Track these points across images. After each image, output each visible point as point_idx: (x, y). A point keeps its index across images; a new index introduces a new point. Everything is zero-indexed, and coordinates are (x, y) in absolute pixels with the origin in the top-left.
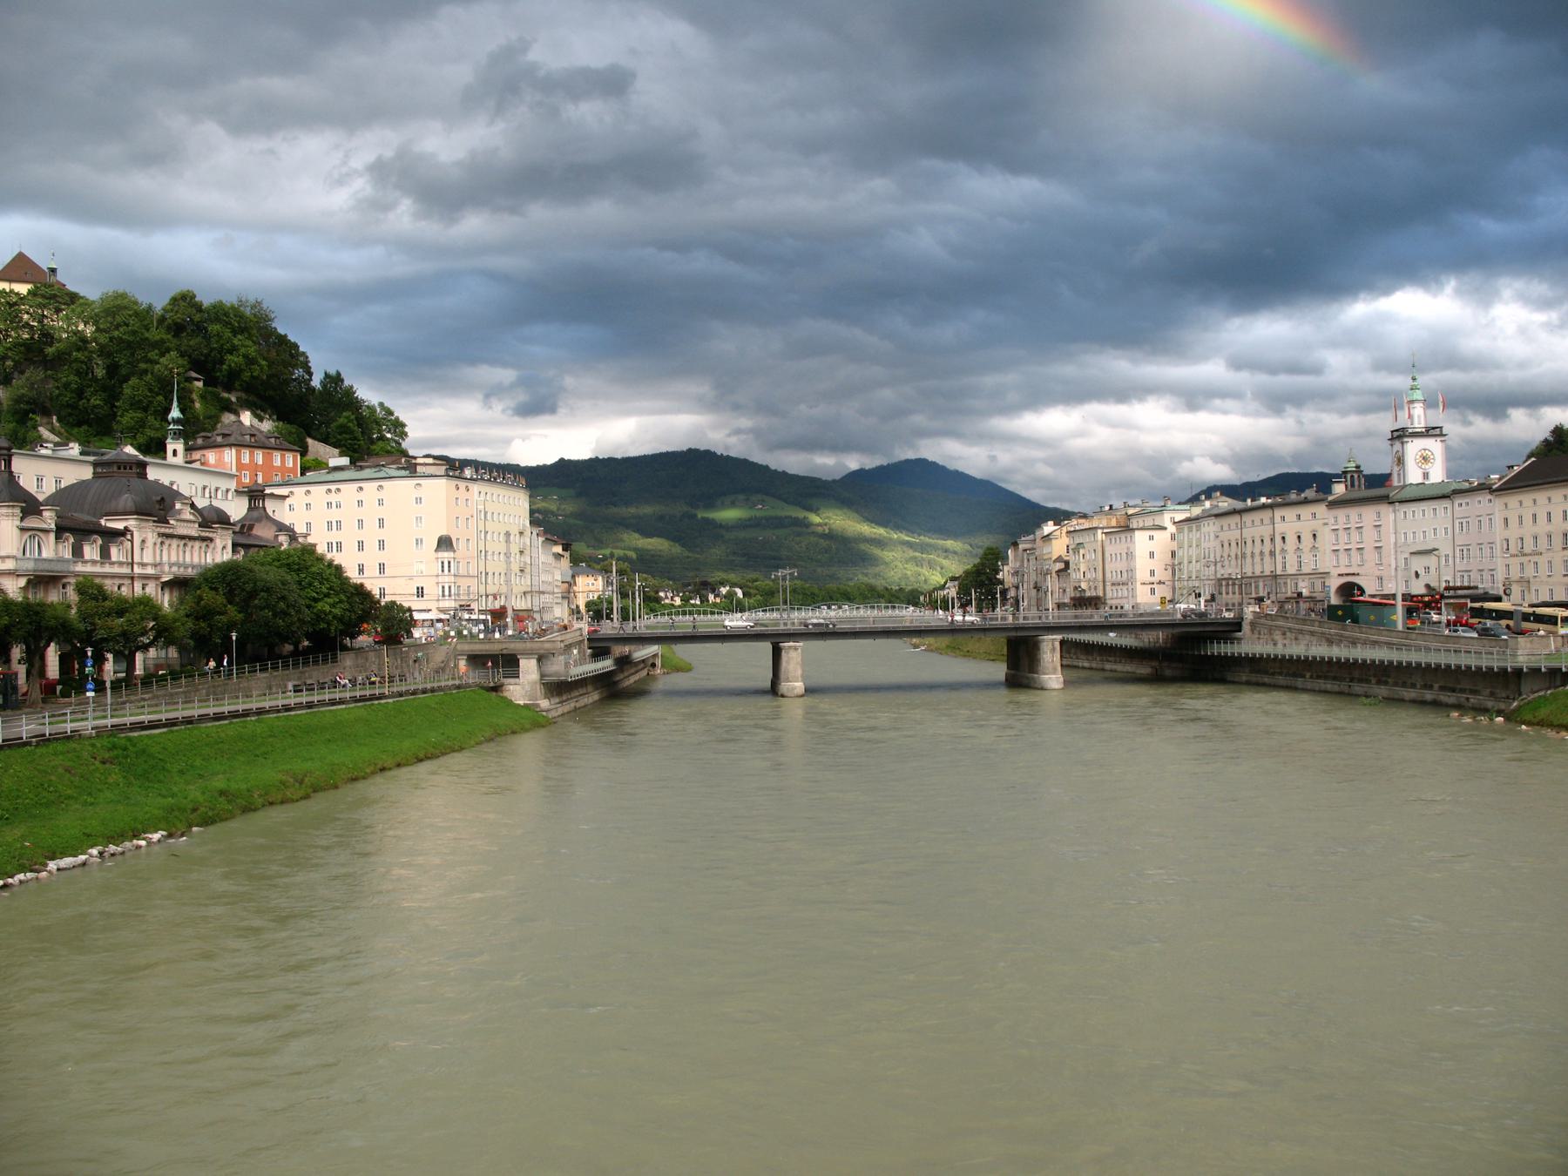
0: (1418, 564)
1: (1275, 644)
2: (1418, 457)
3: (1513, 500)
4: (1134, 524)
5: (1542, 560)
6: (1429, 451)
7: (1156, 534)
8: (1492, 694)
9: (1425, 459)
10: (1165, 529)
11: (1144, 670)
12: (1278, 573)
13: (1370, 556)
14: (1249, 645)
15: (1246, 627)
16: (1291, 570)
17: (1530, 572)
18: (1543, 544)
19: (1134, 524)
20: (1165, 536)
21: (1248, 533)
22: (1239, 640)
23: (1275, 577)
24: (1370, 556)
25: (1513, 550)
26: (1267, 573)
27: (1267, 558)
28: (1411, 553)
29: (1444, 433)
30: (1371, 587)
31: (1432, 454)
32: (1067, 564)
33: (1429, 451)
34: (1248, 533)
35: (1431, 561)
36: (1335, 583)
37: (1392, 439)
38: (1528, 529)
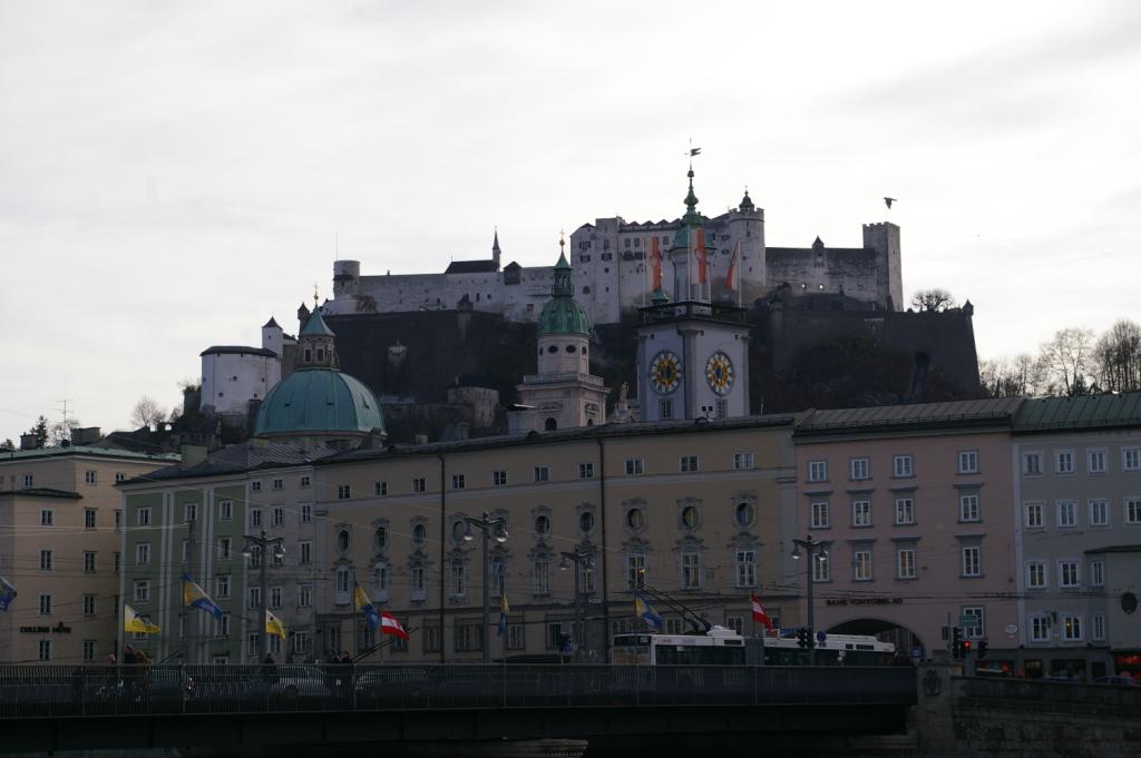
2: (710, 367)
6: (726, 357)
7: (58, 509)
9: (719, 372)
10: (77, 497)
12: (611, 598)
20: (76, 511)
28: (1086, 553)
31: (731, 365)
33: (726, 357)
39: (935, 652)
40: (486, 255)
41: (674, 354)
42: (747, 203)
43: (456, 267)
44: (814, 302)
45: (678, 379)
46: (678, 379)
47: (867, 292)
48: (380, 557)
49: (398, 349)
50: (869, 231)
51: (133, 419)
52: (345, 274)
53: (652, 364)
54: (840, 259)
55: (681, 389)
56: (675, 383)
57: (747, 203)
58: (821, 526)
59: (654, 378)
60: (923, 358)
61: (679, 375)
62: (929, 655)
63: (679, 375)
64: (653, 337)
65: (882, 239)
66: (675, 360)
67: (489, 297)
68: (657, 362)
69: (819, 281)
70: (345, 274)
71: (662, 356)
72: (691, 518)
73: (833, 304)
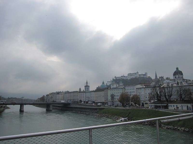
0: (87, 98)
1: (73, 106)
3: (96, 93)
4: (60, 93)
5: (98, 98)
8: (94, 111)
11: (60, 108)
13: (83, 97)
14: (72, 106)
15: (71, 104)
16: (75, 99)
17: (97, 99)
18: (98, 97)
19: (60, 93)
21: (71, 95)
22: (70, 105)
23: (73, 99)
24: (83, 97)
25: (96, 97)
26: (73, 99)
27: (73, 97)
32: (52, 97)
34: (71, 95)
35: (88, 98)
36: (79, 100)
37: (85, 86)
38: (97, 95)
40: (123, 76)
42: (137, 72)
43: (121, 76)
44: (142, 77)
47: (145, 77)
49: (118, 81)
50: (145, 73)
51: (67, 91)
52: (115, 77)
54: (143, 75)
57: (137, 72)
60: (148, 81)
65: (146, 73)
67: (123, 78)
69: (142, 76)
70: (115, 77)
73: (143, 77)
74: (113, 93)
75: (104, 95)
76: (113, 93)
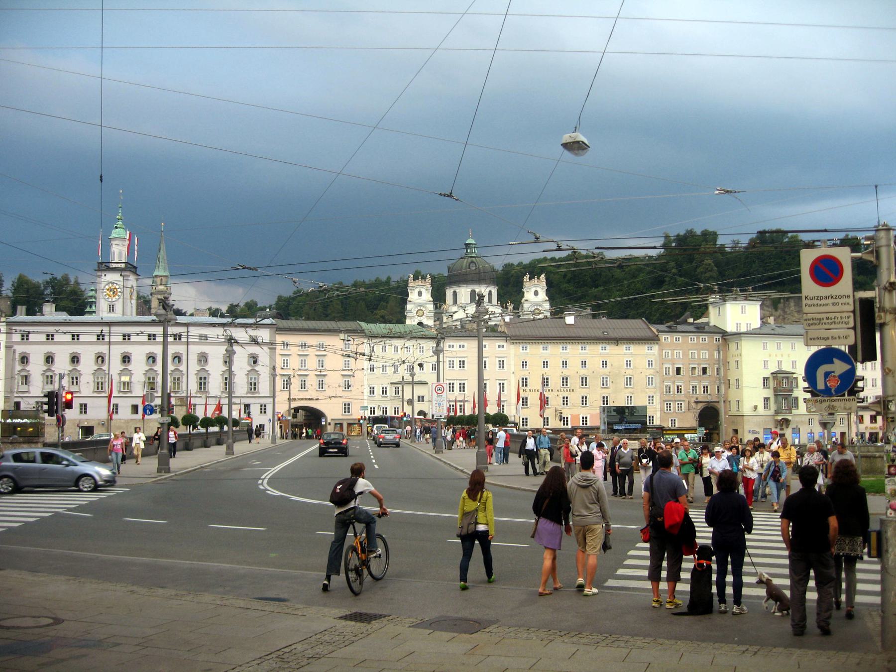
29: (138, 273)
30: (332, 411)
39: (332, 419)
41: (117, 284)
45: (119, 296)
46: (119, 296)
48: (49, 370)
53: (105, 287)
55: (121, 300)
56: (117, 297)
58: (347, 368)
59: (105, 294)
61: (119, 294)
62: (329, 421)
63: (119, 294)
64: (105, 275)
66: (117, 287)
68: (107, 287)
71: (110, 285)
72: (252, 360)
74: (780, 363)
75: (650, 371)
76: (780, 363)
